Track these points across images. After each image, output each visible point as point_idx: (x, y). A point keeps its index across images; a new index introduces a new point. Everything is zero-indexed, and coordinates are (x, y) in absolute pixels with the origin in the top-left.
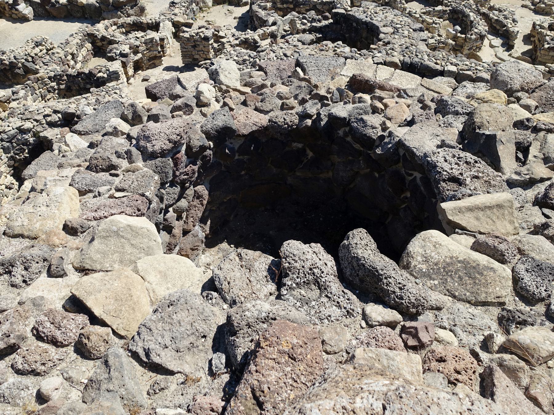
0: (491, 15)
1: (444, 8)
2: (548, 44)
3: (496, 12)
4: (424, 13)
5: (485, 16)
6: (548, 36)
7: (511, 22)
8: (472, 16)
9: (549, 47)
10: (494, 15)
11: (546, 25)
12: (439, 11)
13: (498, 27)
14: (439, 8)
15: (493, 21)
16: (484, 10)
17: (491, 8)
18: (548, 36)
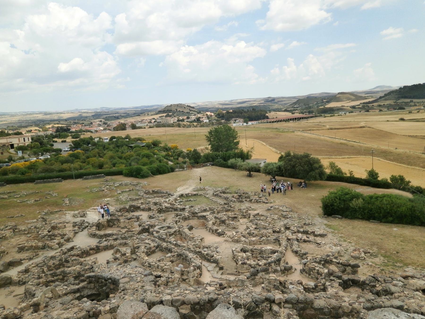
0: (203, 252)
1: (173, 254)
2: (241, 261)
3: (206, 249)
4: (159, 261)
5: (199, 254)
6: (240, 256)
7: (216, 253)
8: (190, 255)
9: (242, 264)
10: (205, 252)
11: (239, 249)
12: (170, 257)
13: (209, 258)
14: (169, 255)
15: (205, 255)
16: (198, 250)
17: (204, 247)
18: (240, 256)
